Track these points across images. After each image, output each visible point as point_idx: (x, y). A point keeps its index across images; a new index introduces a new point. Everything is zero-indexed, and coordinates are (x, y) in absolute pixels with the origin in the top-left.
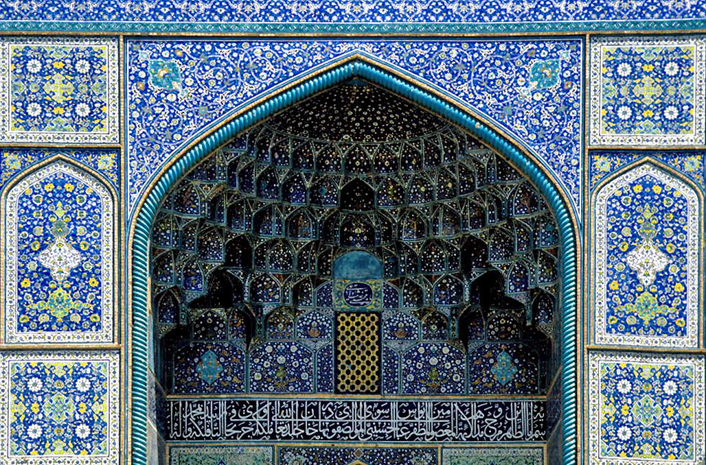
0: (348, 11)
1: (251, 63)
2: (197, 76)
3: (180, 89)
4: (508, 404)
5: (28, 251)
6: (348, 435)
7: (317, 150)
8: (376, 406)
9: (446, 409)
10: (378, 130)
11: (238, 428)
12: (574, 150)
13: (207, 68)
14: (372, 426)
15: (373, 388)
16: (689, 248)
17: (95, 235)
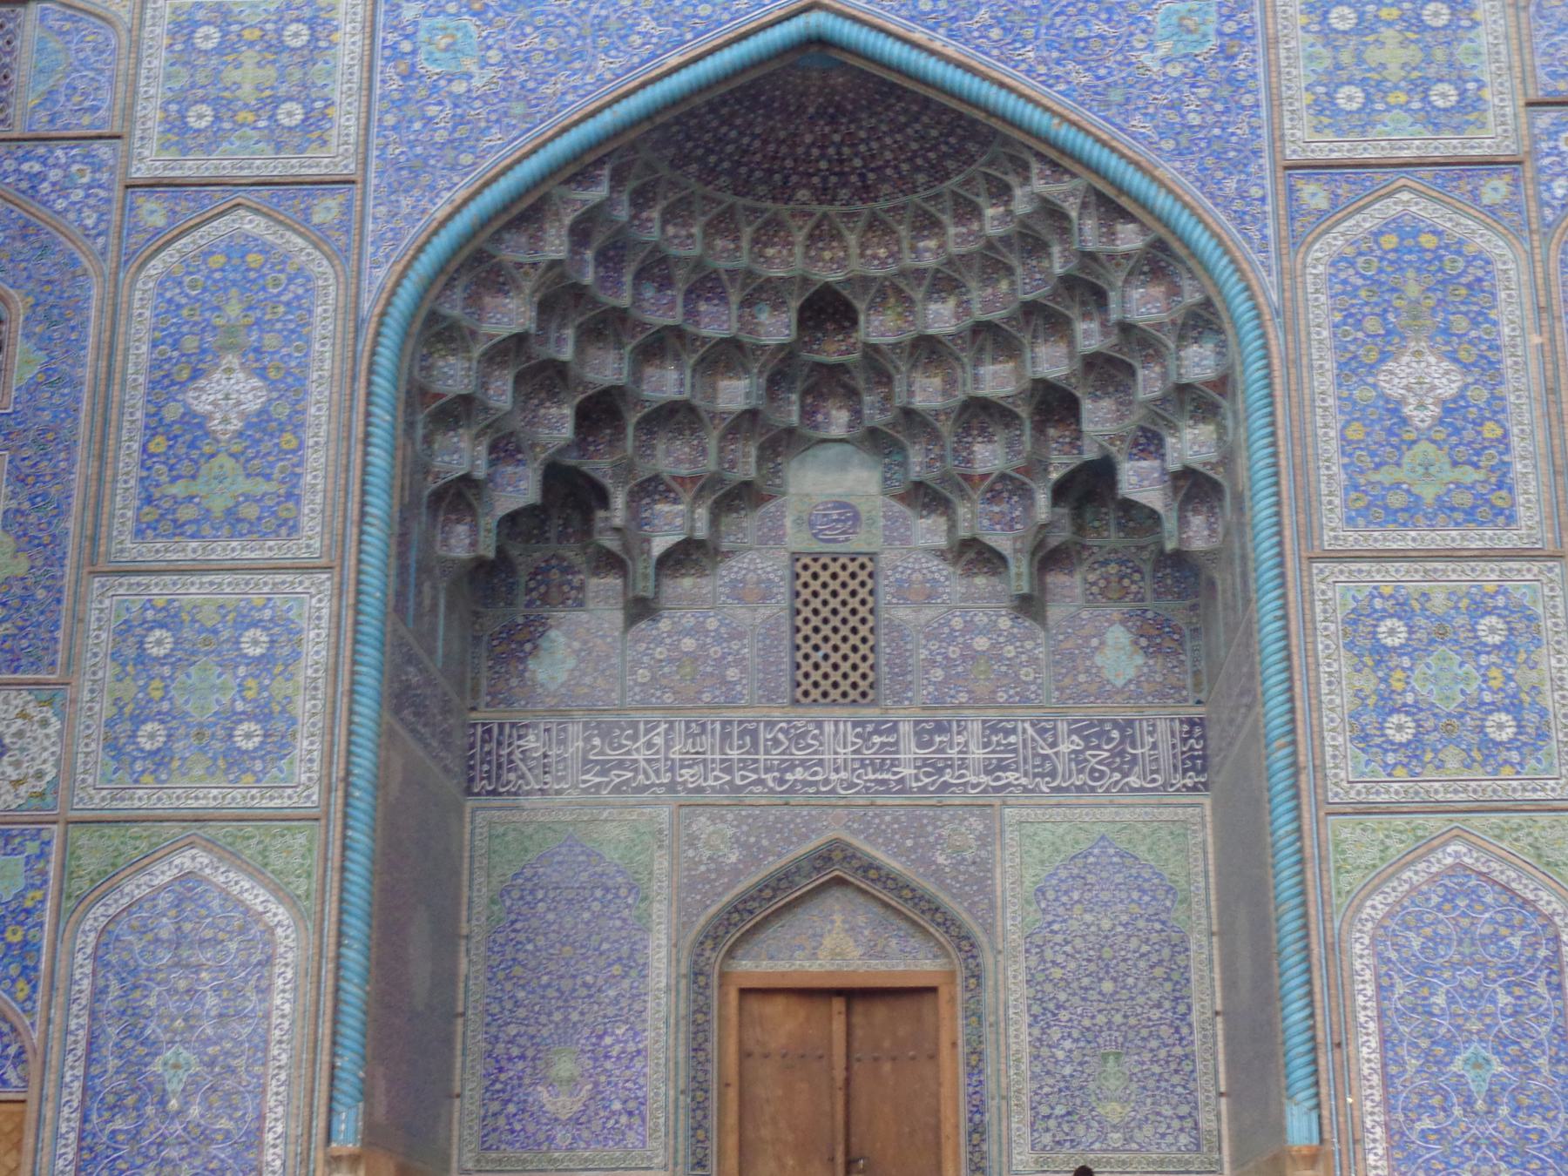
1: (613, 17)
3: (474, 69)
4: (1130, 723)
5: (166, 382)
6: (815, 783)
7: (749, 224)
8: (870, 728)
9: (1008, 733)
10: (862, 177)
11: (604, 773)
12: (1252, 168)
13: (528, 30)
14: (863, 766)
15: (864, 695)
16: (1505, 353)
17: (298, 349)
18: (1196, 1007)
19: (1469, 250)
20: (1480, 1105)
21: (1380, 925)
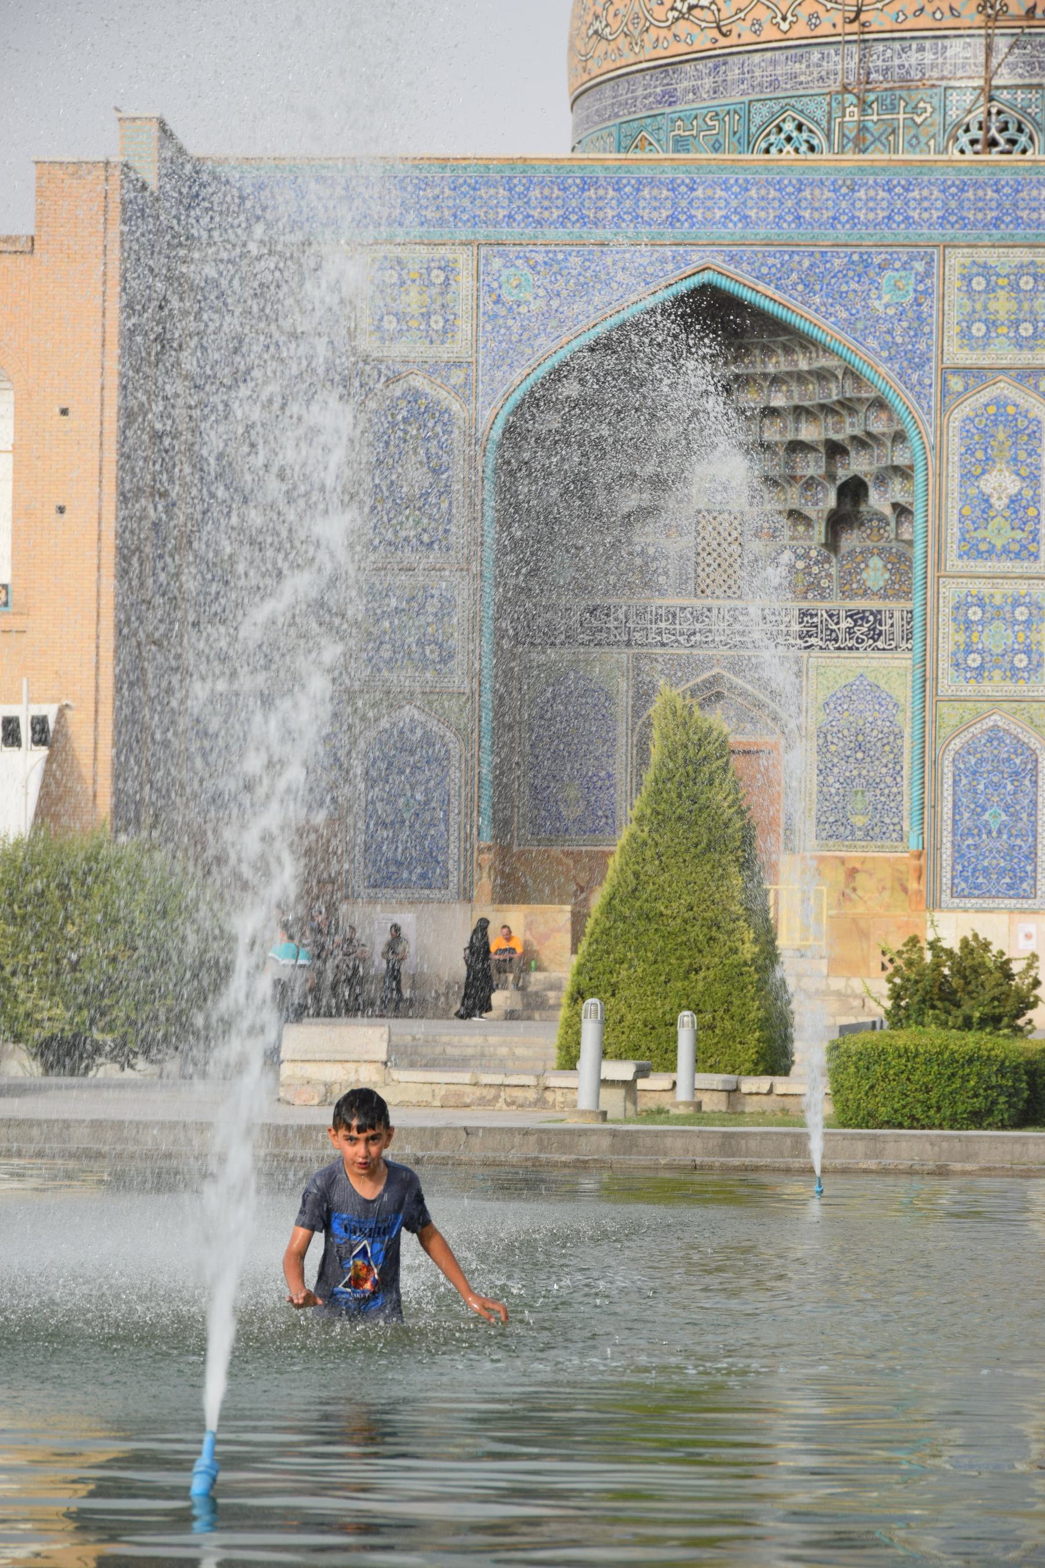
0: (700, 217)
2: (550, 287)
4: (879, 612)
9: (812, 616)
12: (927, 368)
18: (906, 767)
19: (1031, 415)
20: (994, 834)
21: (957, 753)
